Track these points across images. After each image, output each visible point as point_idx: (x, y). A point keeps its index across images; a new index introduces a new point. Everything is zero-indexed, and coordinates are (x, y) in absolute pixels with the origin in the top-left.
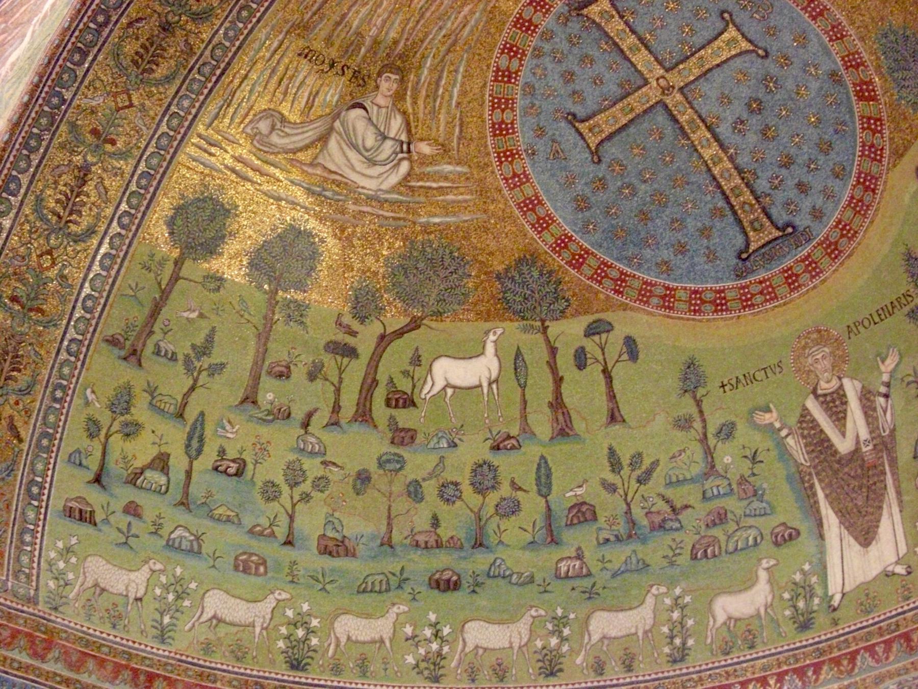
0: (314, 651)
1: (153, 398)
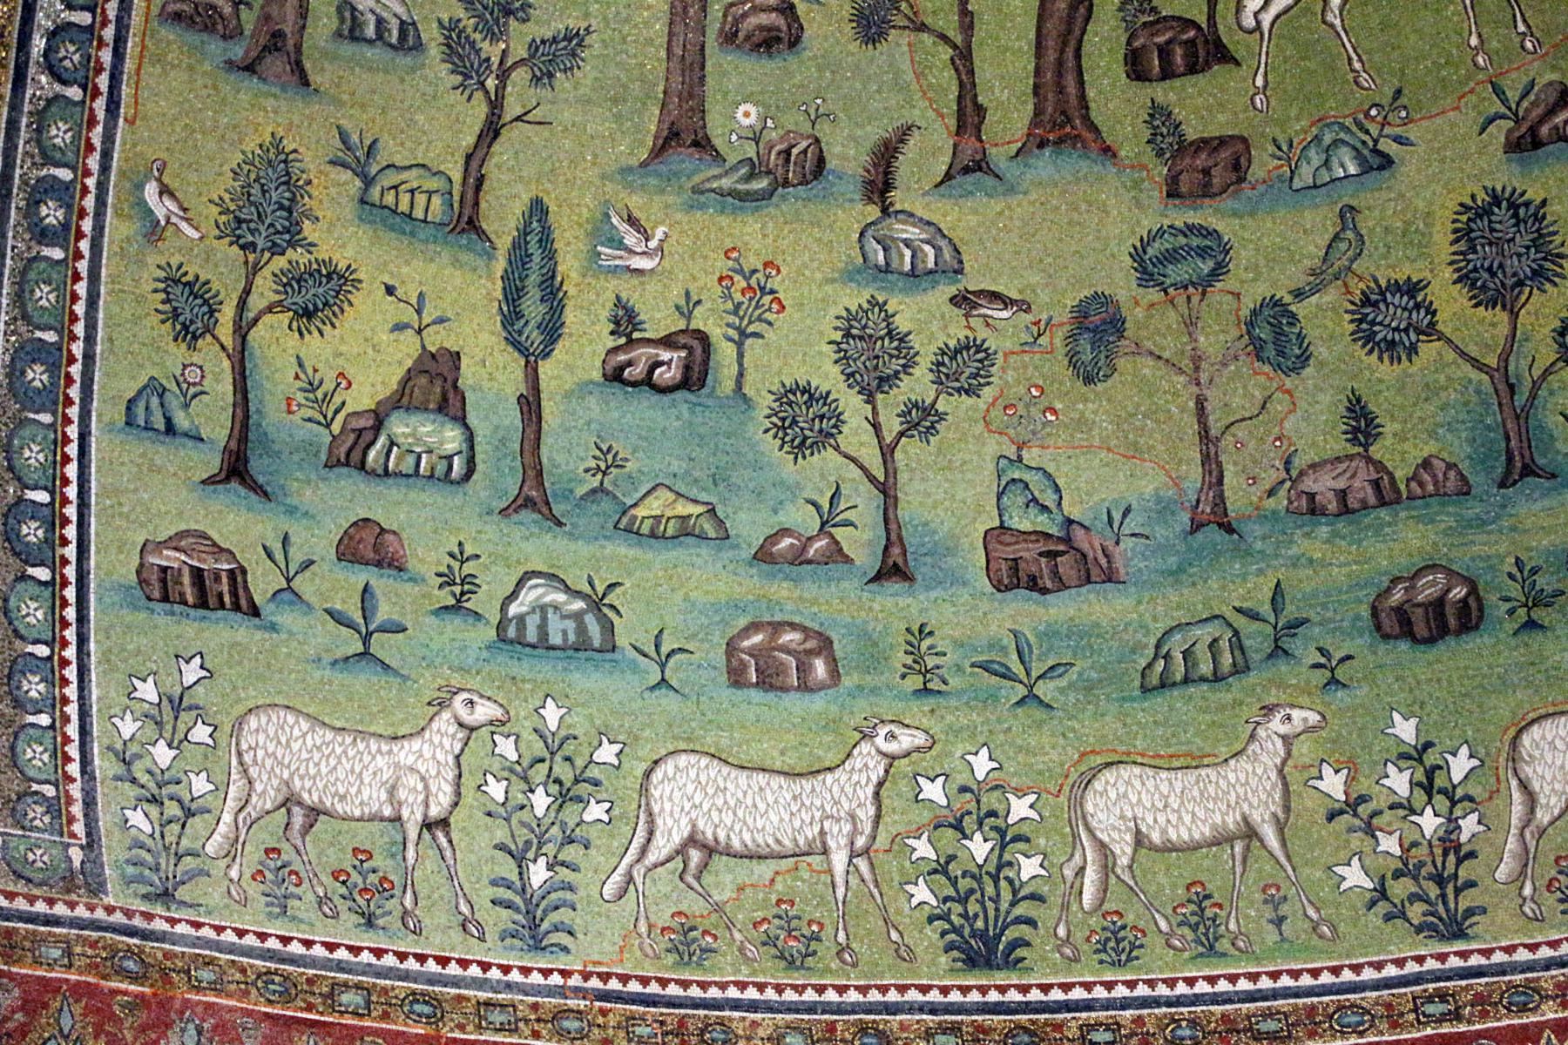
0: (1034, 897)
1: (368, 182)
